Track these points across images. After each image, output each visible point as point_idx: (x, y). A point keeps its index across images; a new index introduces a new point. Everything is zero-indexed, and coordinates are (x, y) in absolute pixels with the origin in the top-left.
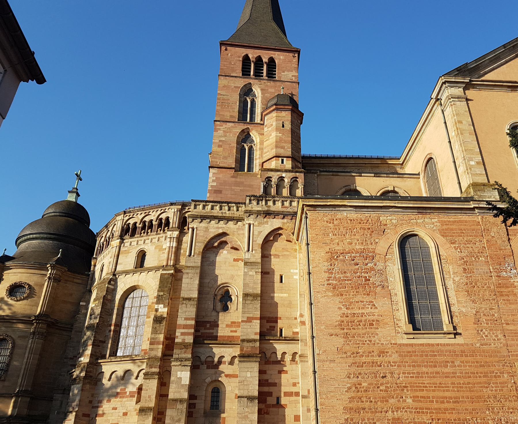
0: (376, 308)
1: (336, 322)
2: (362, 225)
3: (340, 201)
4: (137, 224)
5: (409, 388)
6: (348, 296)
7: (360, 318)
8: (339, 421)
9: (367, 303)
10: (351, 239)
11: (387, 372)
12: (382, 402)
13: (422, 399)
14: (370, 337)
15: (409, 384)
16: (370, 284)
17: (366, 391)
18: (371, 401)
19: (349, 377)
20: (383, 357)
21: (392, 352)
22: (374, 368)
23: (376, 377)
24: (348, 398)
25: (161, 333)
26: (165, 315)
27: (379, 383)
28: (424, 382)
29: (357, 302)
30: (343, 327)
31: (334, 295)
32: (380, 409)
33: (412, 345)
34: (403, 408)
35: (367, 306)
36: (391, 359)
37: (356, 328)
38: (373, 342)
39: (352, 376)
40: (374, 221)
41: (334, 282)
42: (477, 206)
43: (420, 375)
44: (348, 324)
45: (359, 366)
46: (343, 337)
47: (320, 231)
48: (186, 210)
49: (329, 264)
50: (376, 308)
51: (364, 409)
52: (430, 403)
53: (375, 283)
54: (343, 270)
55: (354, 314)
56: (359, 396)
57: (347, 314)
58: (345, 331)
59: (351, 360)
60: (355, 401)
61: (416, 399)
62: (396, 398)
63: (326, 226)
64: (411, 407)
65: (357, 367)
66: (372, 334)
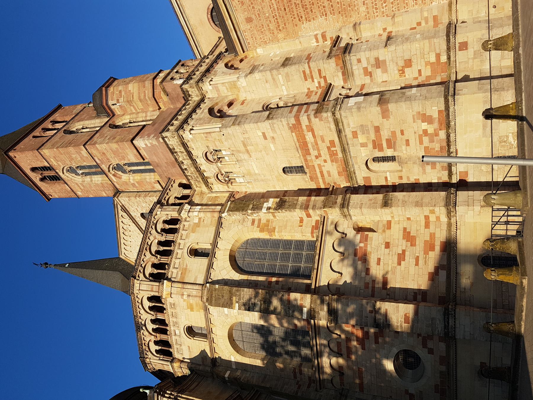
4: (153, 318)
25: (298, 200)
48: (165, 202)
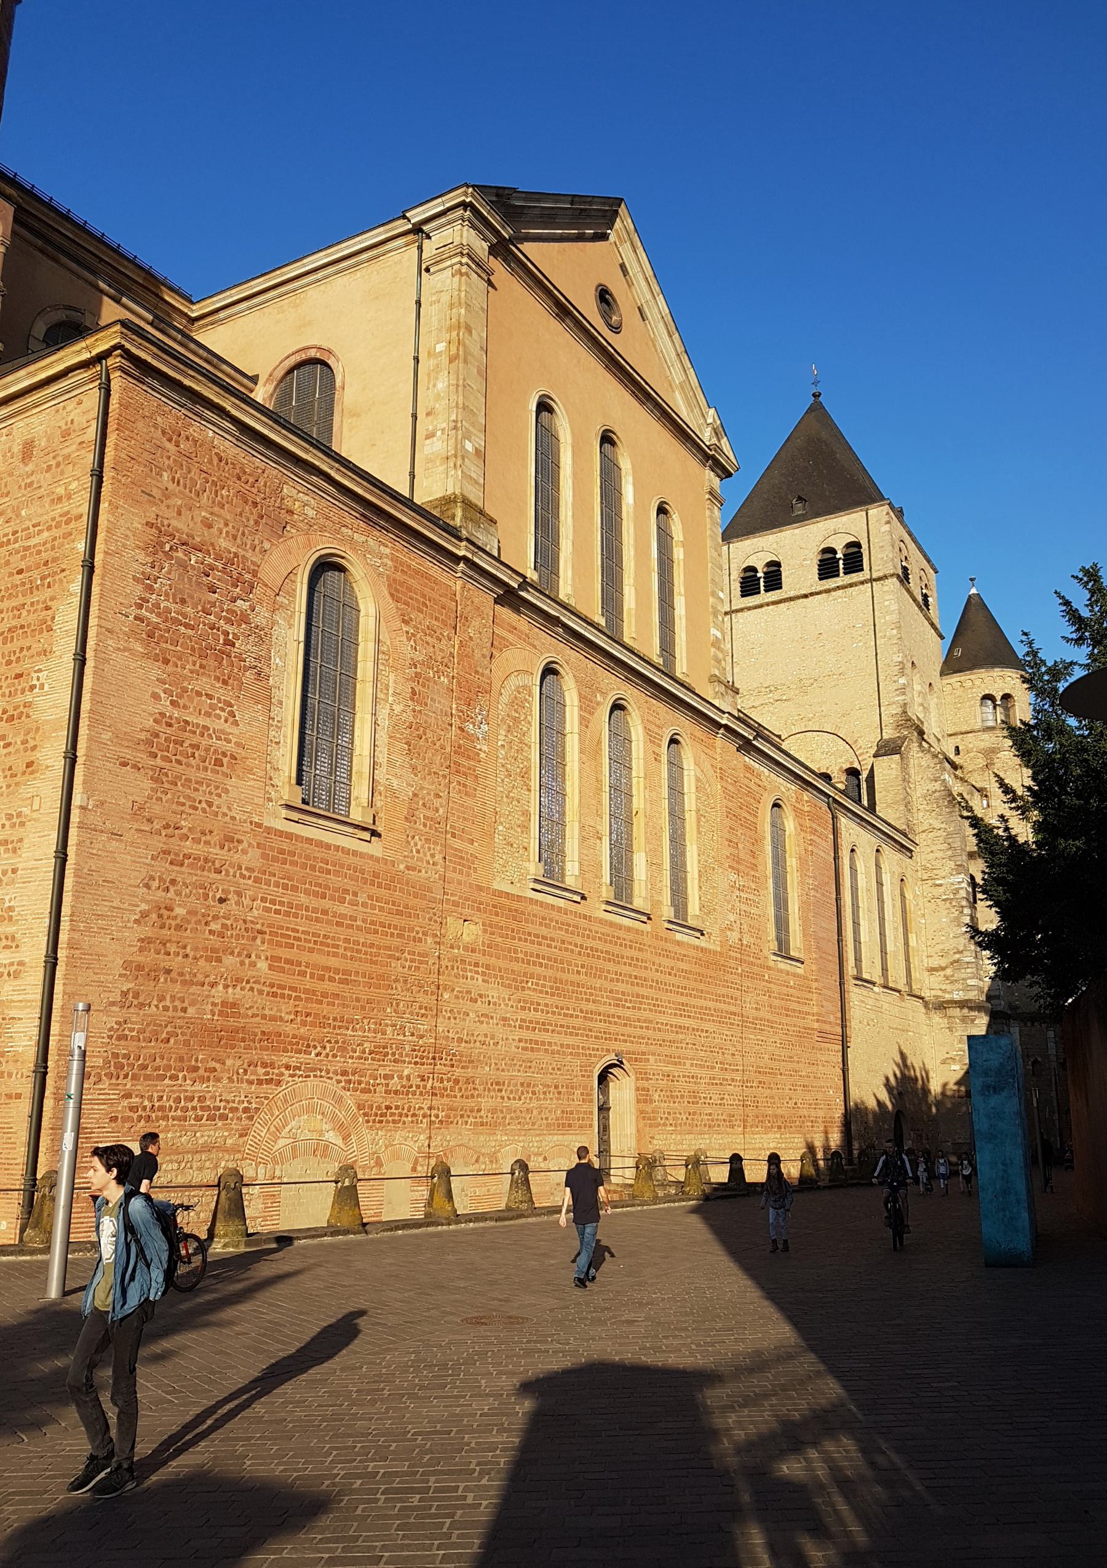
0: (236, 723)
1: (142, 730)
2: (243, 485)
3: (217, 389)
5: (267, 937)
6: (179, 670)
7: (196, 739)
8: (107, 995)
9: (220, 705)
10: (212, 513)
11: (232, 889)
12: (209, 960)
13: (287, 966)
14: (210, 793)
15: (269, 926)
16: (233, 655)
17: (179, 927)
18: (187, 956)
19: (148, 886)
20: (229, 851)
21: (250, 845)
22: (206, 873)
23: (206, 897)
24: (138, 941)
27: (211, 915)
28: (297, 927)
29: (199, 694)
30: (154, 750)
31: (146, 656)
32: (200, 978)
33: (289, 836)
34: (248, 982)
35: (218, 712)
36: (245, 860)
37: (184, 760)
38: (214, 808)
39: (155, 884)
40: (269, 487)
41: (154, 619)
42: (470, 556)
43: (293, 910)
44: (168, 746)
45: (175, 862)
46: (152, 778)
47: (141, 450)
49: (150, 560)
50: (236, 723)
51: (168, 972)
52: (299, 978)
53: (244, 656)
54: (182, 592)
55: (186, 722)
56: (162, 938)
57: (171, 717)
58: (159, 762)
59: (158, 843)
60: (152, 950)
61: (275, 964)
62: (238, 956)
63: (158, 443)
64: (263, 981)
65: (171, 863)
66: (217, 788)
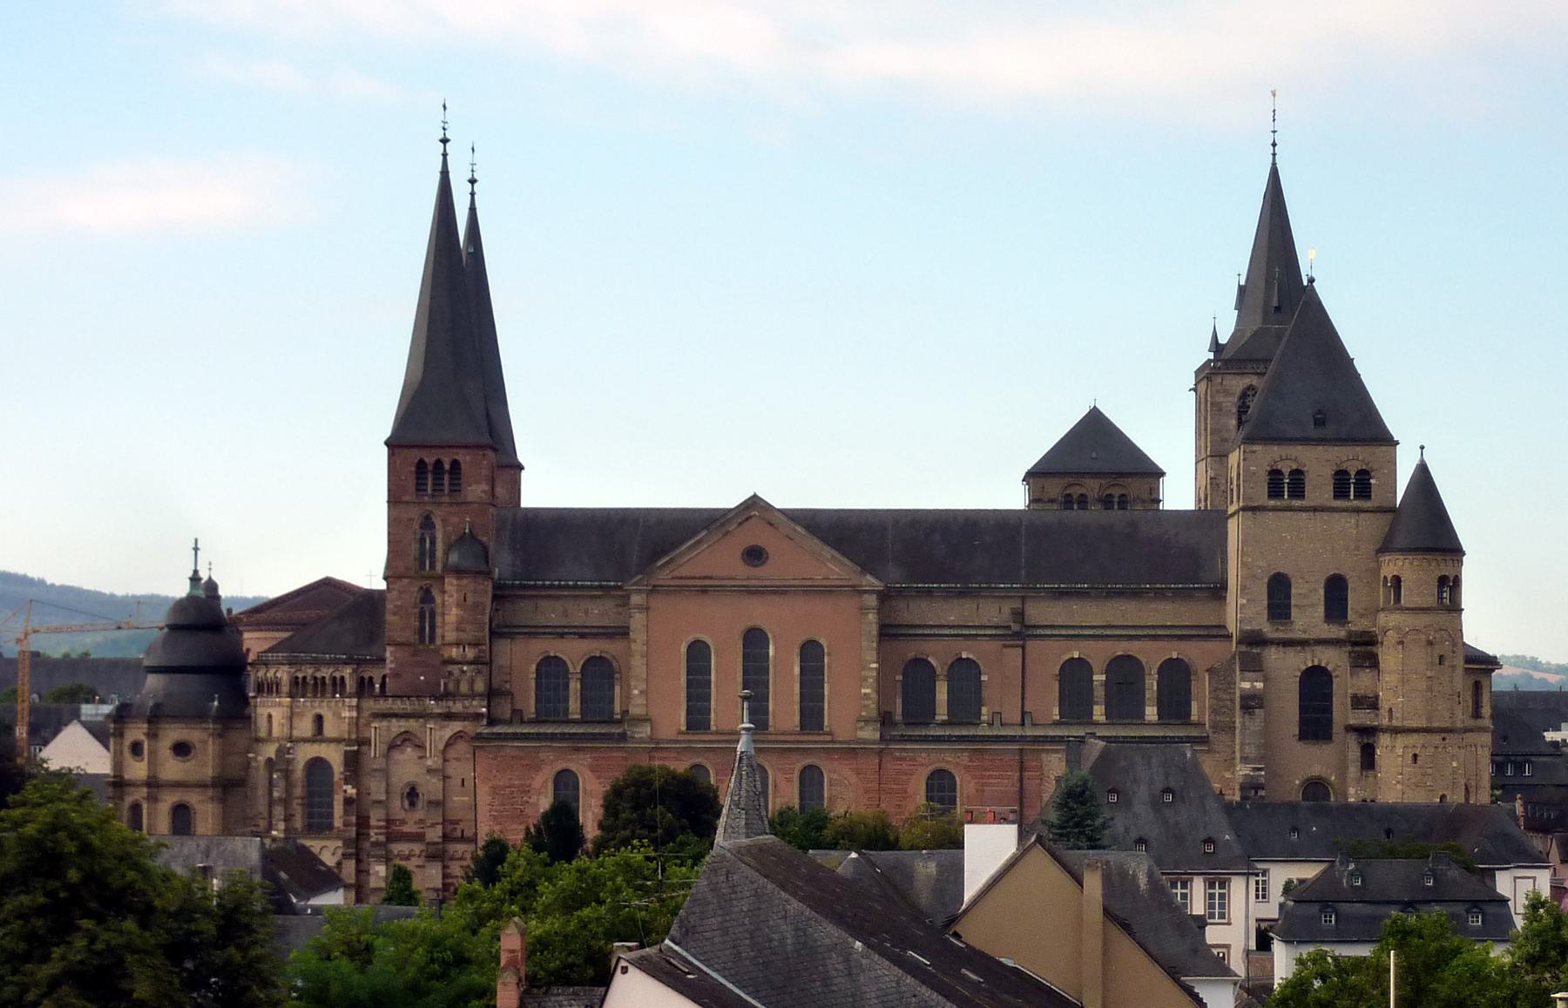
25: (353, 815)
26: (355, 797)
